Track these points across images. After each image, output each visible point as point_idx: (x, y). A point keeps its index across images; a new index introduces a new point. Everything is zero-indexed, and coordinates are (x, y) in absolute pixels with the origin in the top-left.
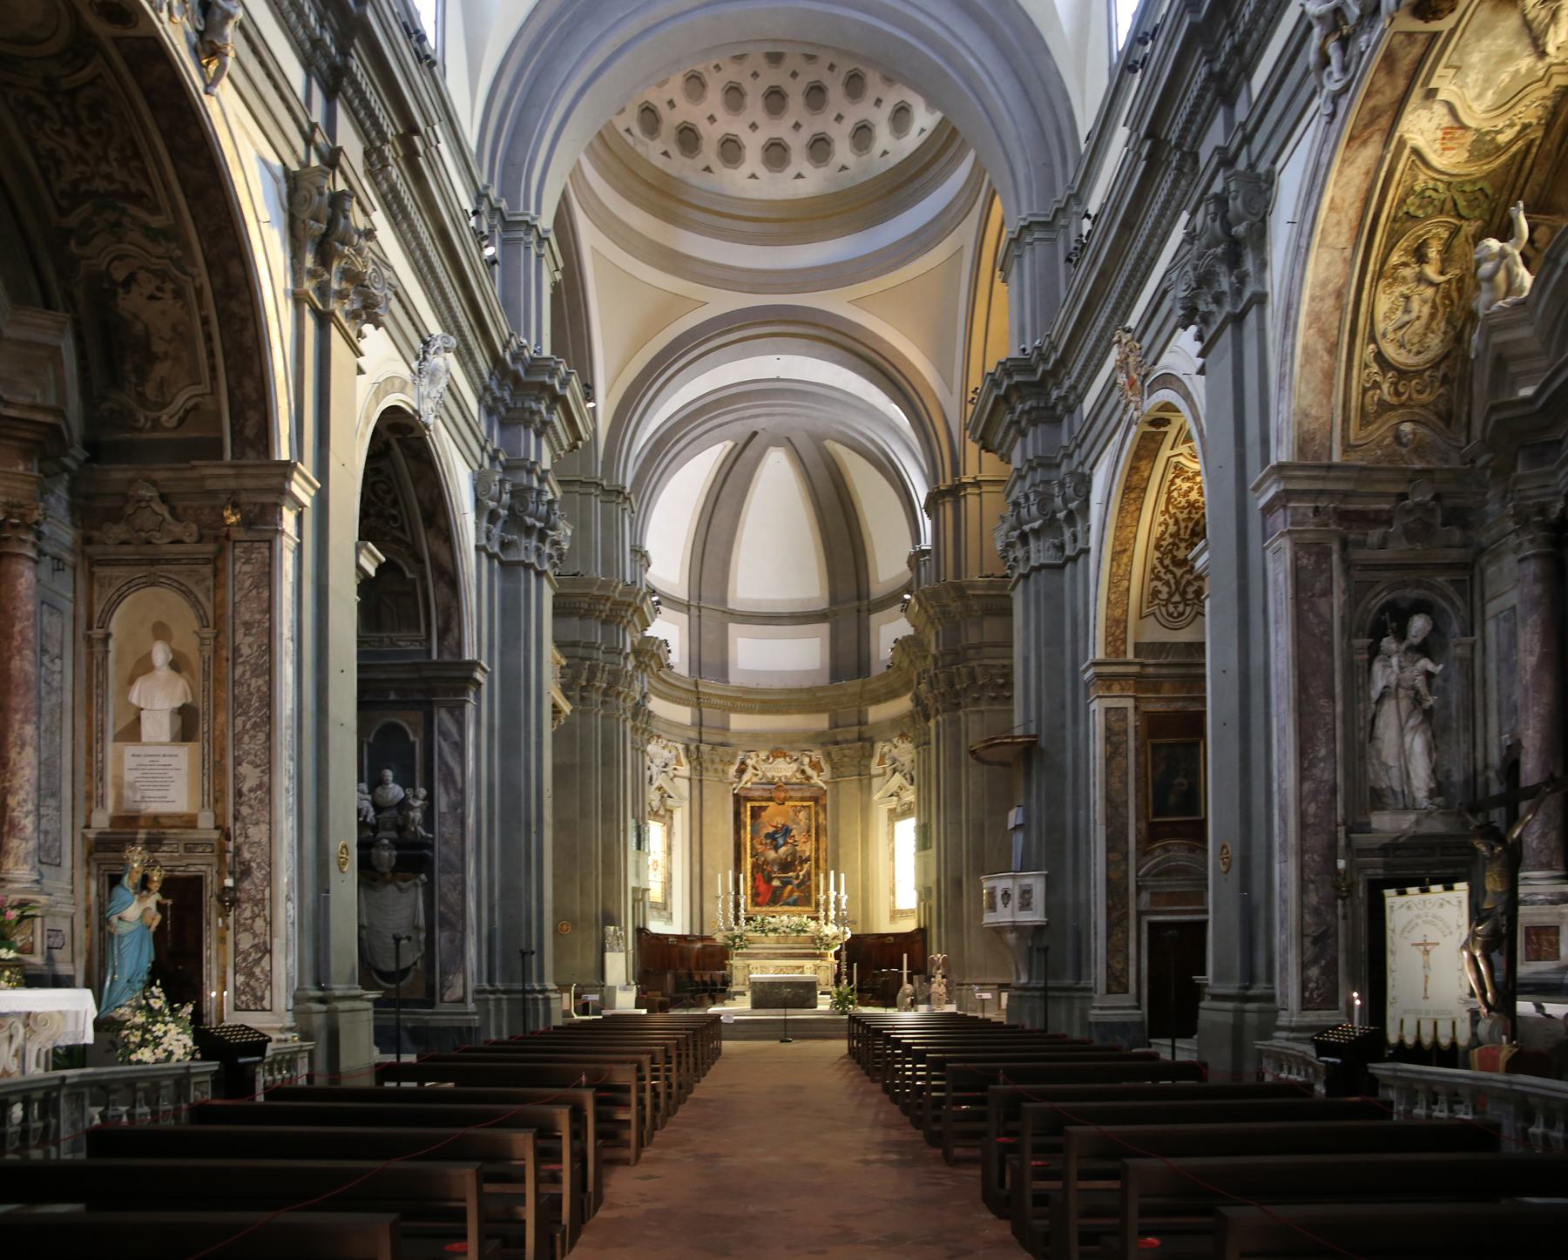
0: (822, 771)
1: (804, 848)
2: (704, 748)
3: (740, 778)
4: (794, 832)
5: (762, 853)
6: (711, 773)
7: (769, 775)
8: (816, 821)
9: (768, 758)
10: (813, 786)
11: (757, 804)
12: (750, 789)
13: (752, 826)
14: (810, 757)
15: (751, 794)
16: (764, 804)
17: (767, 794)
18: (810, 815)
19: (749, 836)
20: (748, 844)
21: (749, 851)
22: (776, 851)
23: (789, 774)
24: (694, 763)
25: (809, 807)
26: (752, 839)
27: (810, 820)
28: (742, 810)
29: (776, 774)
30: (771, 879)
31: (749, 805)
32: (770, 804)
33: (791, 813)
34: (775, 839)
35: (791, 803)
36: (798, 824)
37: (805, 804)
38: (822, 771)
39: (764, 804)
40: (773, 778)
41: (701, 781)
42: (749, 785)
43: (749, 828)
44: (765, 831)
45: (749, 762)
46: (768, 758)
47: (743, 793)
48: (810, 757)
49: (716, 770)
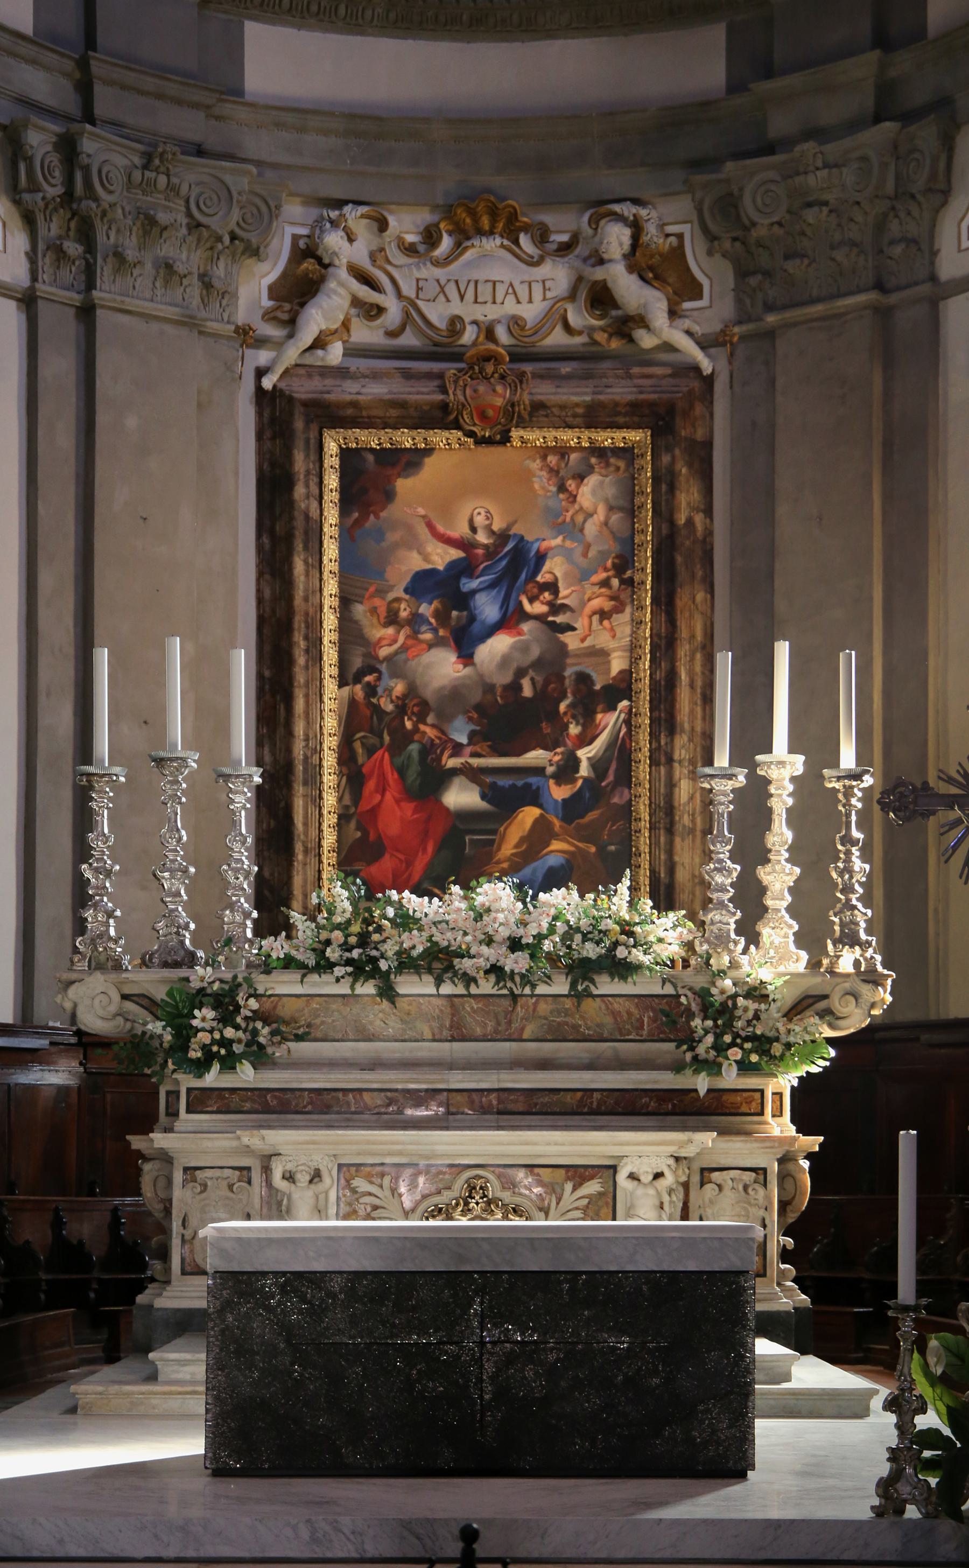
0: (695, 291)
1: (602, 639)
2: (91, 144)
3: (291, 324)
4: (554, 568)
5: (396, 665)
6: (145, 276)
7: (437, 314)
8: (664, 513)
9: (431, 237)
10: (645, 357)
11: (372, 439)
12: (341, 373)
13: (347, 537)
14: (636, 227)
15: (348, 391)
16: (406, 439)
17: (425, 394)
18: (630, 490)
19: (331, 586)
20: (330, 621)
21: (330, 655)
22: (466, 657)
23: (531, 312)
24: (52, 228)
25: (627, 453)
26: (345, 602)
27: (632, 512)
28: (300, 462)
29: (468, 311)
30: (443, 778)
31: (331, 447)
32: (439, 438)
33: (542, 483)
34: (463, 601)
35: (535, 436)
36: (573, 530)
37: (606, 438)
38: (695, 291)
39: (406, 439)
40: (455, 326)
41: (87, 313)
42: (335, 354)
43: (331, 550)
44: (414, 563)
45: (334, 240)
46: (431, 237)
47: (303, 389)
48: (636, 227)
49: (167, 269)
